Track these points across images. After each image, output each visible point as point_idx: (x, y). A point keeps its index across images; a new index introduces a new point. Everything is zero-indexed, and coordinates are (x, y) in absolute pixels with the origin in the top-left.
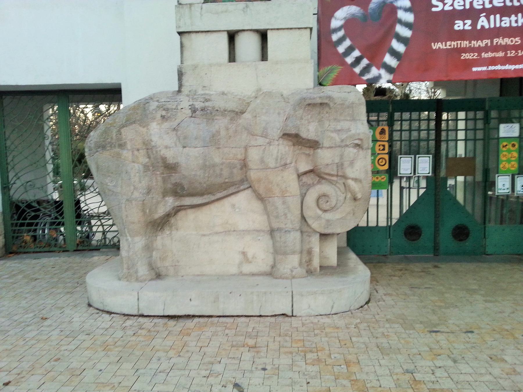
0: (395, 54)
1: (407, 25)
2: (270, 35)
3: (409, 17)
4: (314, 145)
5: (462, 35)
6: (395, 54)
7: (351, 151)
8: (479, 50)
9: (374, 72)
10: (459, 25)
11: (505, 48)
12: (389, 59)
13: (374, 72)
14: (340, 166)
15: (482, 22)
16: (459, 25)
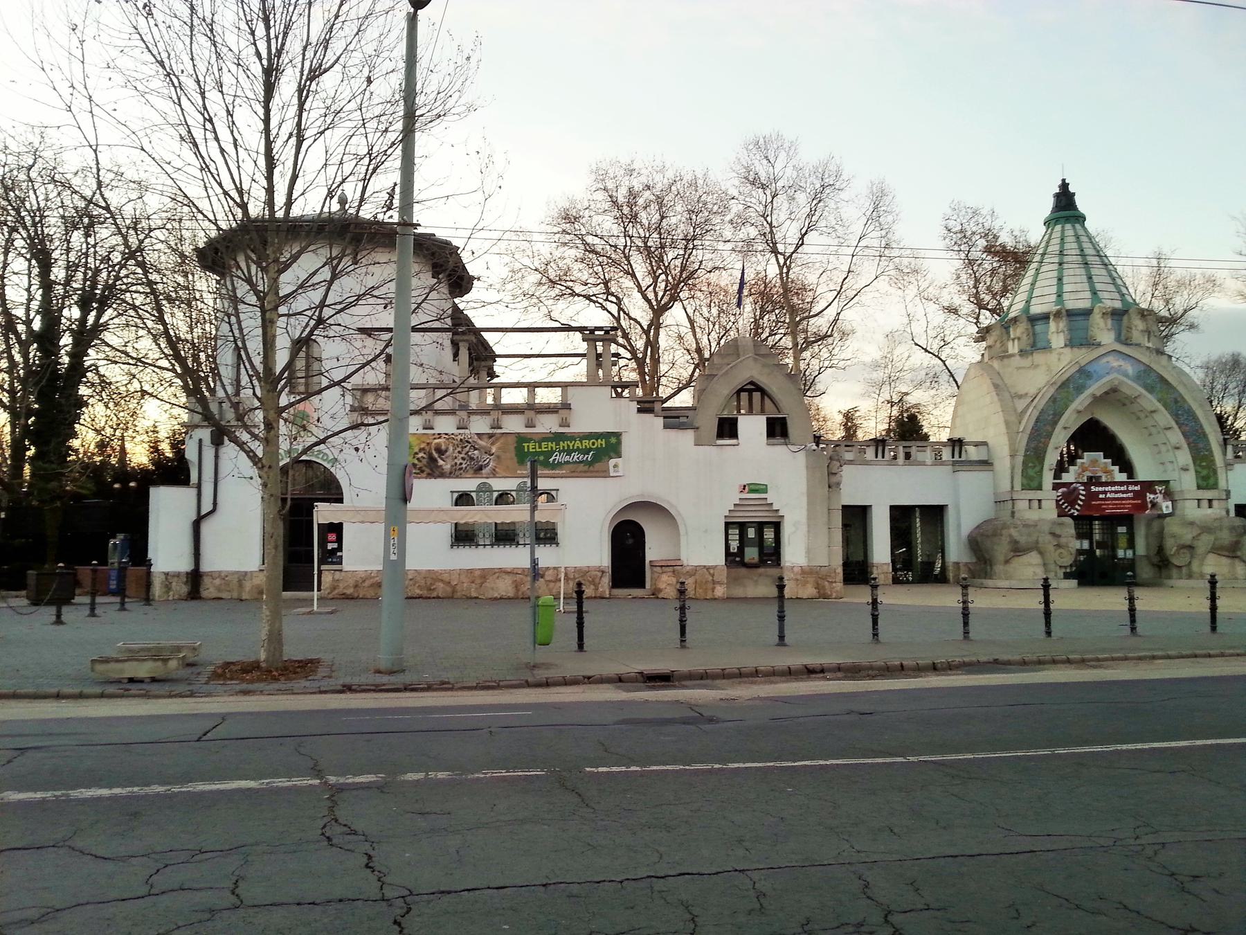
0: (1079, 505)
1: (1083, 495)
2: (1043, 502)
3: (1084, 493)
4: (1059, 536)
5: (1102, 499)
6: (1079, 505)
7: (1071, 539)
8: (1108, 504)
9: (1072, 511)
10: (1101, 496)
11: (1116, 504)
12: (1077, 507)
13: (1072, 511)
14: (1067, 543)
15: (1108, 495)
16: (1101, 496)
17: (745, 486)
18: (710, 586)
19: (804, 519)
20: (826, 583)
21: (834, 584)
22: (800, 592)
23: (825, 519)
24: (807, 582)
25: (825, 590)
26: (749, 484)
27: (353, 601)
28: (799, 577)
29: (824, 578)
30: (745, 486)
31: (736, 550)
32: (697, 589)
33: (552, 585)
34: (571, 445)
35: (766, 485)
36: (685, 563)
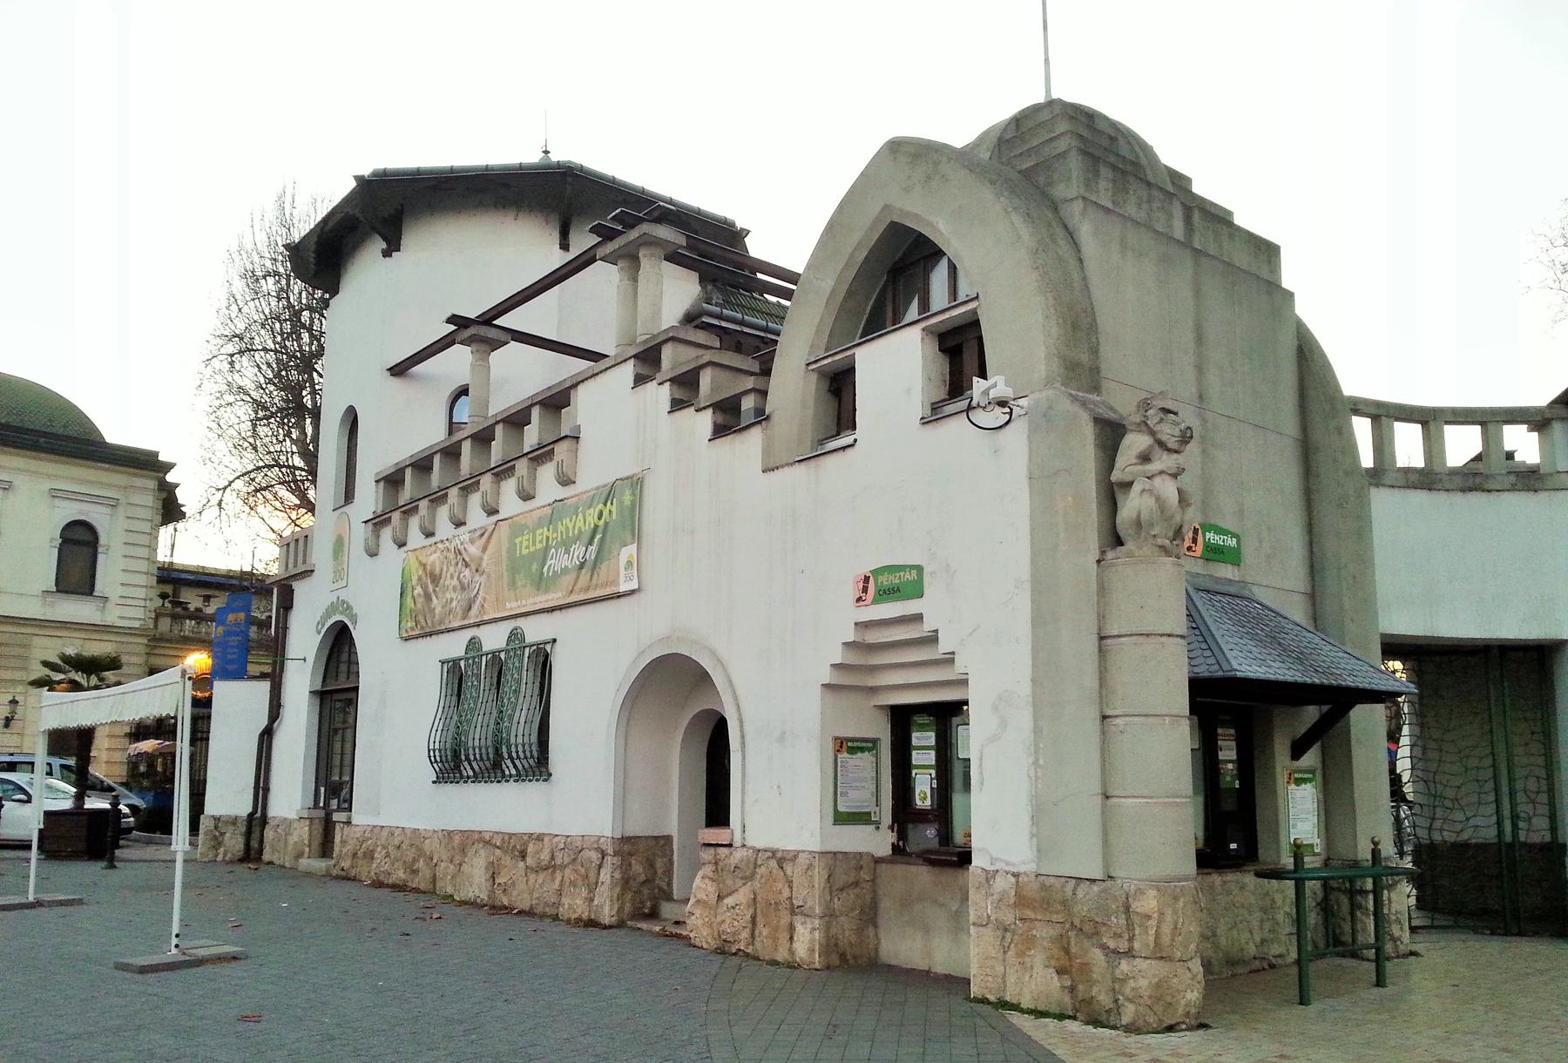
17: (867, 579)
18: (785, 919)
19: (1025, 689)
20: (1097, 956)
21: (1124, 966)
22: (1011, 979)
23: (1091, 681)
24: (1030, 942)
25: (1091, 983)
26: (876, 572)
27: (349, 882)
28: (1009, 917)
29: (1091, 930)
30: (867, 579)
31: (928, 802)
32: (760, 926)
33: (532, 877)
34: (570, 525)
35: (919, 569)
36: (737, 842)
